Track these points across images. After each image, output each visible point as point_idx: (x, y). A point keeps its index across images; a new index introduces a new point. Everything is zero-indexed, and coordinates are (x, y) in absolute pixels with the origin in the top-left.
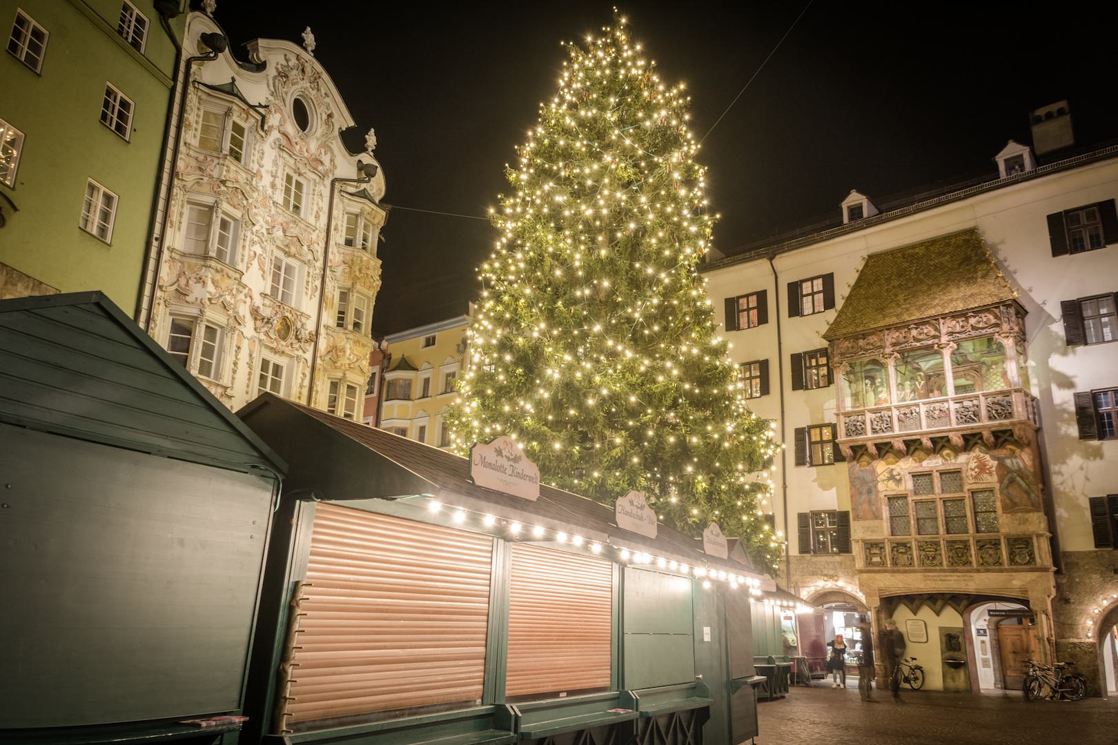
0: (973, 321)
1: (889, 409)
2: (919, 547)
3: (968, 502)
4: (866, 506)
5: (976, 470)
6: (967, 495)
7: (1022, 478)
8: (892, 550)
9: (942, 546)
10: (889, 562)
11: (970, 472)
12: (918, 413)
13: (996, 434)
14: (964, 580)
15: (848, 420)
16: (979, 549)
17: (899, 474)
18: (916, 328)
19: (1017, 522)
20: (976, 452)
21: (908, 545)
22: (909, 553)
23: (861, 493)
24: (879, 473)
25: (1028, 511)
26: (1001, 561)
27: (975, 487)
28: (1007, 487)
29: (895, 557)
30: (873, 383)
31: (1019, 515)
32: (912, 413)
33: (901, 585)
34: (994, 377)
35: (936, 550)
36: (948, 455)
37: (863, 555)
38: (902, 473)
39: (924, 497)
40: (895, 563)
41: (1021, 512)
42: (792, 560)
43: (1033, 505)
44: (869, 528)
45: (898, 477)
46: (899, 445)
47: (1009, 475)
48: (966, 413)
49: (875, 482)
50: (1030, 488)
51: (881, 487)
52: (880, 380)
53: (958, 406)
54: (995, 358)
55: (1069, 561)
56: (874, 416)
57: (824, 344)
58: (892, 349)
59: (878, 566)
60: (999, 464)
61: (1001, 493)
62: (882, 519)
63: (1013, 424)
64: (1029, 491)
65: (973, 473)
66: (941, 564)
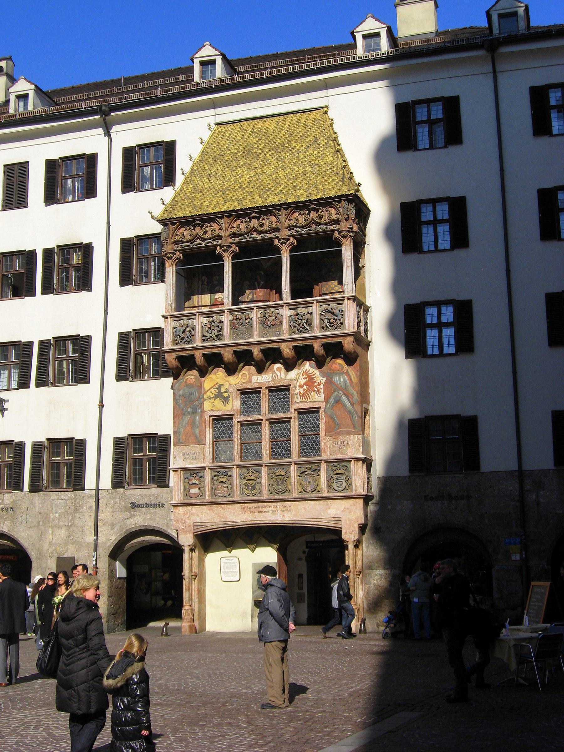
0: (313, 215)
1: (222, 313)
2: (240, 474)
3: (294, 425)
5: (305, 387)
6: (293, 414)
7: (347, 397)
8: (212, 479)
9: (263, 474)
10: (207, 494)
12: (251, 319)
13: (325, 346)
14: (282, 511)
15: (175, 324)
16: (300, 476)
17: (227, 391)
18: (258, 218)
20: (308, 366)
21: (229, 474)
22: (229, 482)
23: (184, 414)
24: (206, 390)
25: (349, 434)
26: (318, 488)
27: (302, 406)
28: (333, 406)
31: (341, 437)
32: (246, 319)
36: (278, 369)
38: (231, 390)
40: (214, 494)
41: (343, 434)
43: (354, 427)
44: (190, 454)
45: (225, 395)
47: (336, 393)
48: (299, 322)
49: (201, 400)
50: (353, 407)
51: (207, 406)
52: (218, 277)
53: (292, 312)
56: (205, 320)
57: (158, 228)
58: (231, 241)
60: (326, 382)
62: (205, 444)
64: (352, 411)
65: (302, 391)
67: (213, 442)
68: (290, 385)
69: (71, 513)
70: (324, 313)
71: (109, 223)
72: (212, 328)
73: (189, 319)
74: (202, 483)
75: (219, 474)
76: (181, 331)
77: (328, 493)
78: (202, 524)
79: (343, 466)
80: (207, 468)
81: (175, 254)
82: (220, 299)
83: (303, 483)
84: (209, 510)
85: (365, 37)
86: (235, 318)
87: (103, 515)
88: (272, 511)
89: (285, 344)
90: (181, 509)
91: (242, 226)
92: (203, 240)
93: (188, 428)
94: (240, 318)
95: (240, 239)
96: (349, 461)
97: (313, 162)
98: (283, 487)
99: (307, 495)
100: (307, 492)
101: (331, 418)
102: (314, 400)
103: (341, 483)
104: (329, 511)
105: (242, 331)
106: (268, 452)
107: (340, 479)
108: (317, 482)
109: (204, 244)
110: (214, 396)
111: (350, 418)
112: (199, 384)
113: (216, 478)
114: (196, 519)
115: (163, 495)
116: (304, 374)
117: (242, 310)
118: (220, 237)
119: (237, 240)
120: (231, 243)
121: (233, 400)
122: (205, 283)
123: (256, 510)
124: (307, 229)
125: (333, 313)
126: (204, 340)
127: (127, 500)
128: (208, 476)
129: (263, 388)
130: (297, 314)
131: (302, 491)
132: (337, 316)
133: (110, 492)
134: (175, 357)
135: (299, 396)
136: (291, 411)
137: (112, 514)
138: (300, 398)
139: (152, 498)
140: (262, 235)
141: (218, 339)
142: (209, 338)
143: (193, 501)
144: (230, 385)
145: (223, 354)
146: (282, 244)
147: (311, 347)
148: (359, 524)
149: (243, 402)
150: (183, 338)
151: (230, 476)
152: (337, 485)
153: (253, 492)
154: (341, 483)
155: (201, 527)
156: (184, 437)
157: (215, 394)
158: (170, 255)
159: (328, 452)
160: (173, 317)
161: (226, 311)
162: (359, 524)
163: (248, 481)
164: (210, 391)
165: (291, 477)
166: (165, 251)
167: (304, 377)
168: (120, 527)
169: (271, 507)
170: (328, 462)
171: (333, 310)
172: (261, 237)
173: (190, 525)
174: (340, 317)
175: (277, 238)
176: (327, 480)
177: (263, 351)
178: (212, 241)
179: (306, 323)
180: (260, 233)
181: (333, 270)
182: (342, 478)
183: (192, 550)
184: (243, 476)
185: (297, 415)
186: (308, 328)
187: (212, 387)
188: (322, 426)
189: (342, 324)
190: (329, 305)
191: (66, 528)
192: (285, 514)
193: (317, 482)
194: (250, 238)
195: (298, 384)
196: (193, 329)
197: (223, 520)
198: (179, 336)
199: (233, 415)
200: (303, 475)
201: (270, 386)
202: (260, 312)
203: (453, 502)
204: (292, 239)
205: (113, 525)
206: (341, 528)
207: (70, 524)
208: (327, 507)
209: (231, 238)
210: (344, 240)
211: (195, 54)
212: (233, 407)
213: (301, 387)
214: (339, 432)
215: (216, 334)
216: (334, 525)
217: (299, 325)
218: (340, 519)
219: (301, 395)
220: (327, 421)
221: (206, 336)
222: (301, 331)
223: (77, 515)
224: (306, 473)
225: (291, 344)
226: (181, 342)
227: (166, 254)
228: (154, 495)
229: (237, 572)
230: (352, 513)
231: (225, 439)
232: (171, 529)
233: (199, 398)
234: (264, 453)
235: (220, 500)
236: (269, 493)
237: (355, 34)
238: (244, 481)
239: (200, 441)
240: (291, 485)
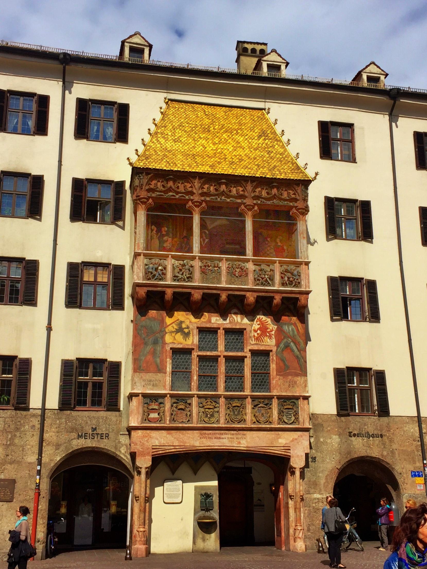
0: (275, 191)
1: (193, 258)
2: (199, 404)
3: (248, 362)
4: (149, 357)
5: (259, 332)
6: (249, 355)
7: (295, 343)
8: (172, 406)
11: (253, 334)
12: (219, 268)
14: (237, 438)
16: (253, 409)
17: (188, 328)
18: (226, 185)
19: (288, 384)
21: (188, 402)
22: (188, 409)
23: (146, 344)
24: (168, 324)
25: (297, 375)
26: (270, 420)
27: (256, 348)
28: (283, 350)
29: (174, 414)
30: (159, 231)
31: (290, 377)
32: (215, 267)
33: (176, 443)
34: (269, 248)
35: (215, 407)
37: (141, 410)
38: (191, 326)
39: (208, 353)
40: (173, 420)
41: (291, 375)
42: (48, 413)
43: (301, 369)
44: (150, 381)
45: (186, 331)
46: (197, 295)
47: (285, 340)
50: (300, 353)
51: (168, 338)
52: (166, 229)
53: (257, 268)
54: (270, 232)
55: (316, 422)
56: (177, 263)
58: (203, 198)
59: (155, 422)
60: (278, 330)
61: (276, 355)
62: (166, 373)
63: (301, 293)
64: (299, 357)
66: (218, 421)
67: (172, 371)
68: (245, 329)
69: (10, 432)
70: (284, 272)
71: (61, 162)
72: (183, 270)
73: (160, 259)
74: (161, 409)
75: (179, 402)
76: (154, 269)
77: (279, 424)
78: (160, 447)
79: (291, 402)
80: (168, 395)
81: (148, 201)
82: (168, 247)
83: (257, 414)
84: (169, 434)
85: (269, 66)
86: (205, 264)
87: (48, 435)
88: (228, 438)
89: (250, 293)
90: (140, 432)
91: (212, 188)
92: (177, 193)
93: (149, 357)
94: (210, 265)
95: (212, 199)
96: (297, 398)
97: (266, 149)
98: (239, 417)
99: (260, 426)
100: (260, 423)
101: (281, 360)
102: (267, 344)
103: (290, 416)
104: (280, 441)
105: (211, 277)
106: (224, 384)
107: (289, 413)
108: (269, 414)
109: (177, 196)
110: (175, 330)
111: (298, 362)
112: (161, 318)
113: (175, 405)
114: (155, 442)
115: (112, 417)
116: (258, 321)
117: (212, 259)
118: (192, 193)
119: (208, 199)
120: (203, 201)
121: (193, 336)
122: (154, 232)
123: (214, 436)
124: (272, 201)
125: (292, 274)
126: (175, 280)
127: (74, 421)
128: (168, 403)
129: (221, 328)
130: (261, 270)
131: (256, 421)
132: (295, 276)
133: (56, 412)
134: (146, 291)
135: (253, 339)
136: (245, 350)
137: (57, 434)
138: (255, 341)
139: (101, 420)
140: (231, 199)
141: (189, 281)
142: (180, 279)
143: (155, 425)
144: (190, 322)
145: (193, 294)
146: (248, 210)
147: (273, 298)
148: (306, 454)
149: (200, 338)
150: (154, 275)
151: (190, 404)
152: (287, 418)
153: (211, 420)
154: (290, 416)
155: (159, 450)
156: (145, 365)
157: (176, 329)
158: (145, 200)
159: (279, 389)
160: (145, 255)
161: (197, 258)
162: (306, 454)
163: (207, 410)
164: (171, 325)
165: (246, 408)
166: (139, 196)
167: (258, 323)
168: (66, 447)
169: (228, 434)
170: (279, 398)
171: (292, 270)
172: (230, 200)
173: (149, 448)
174: (298, 277)
175: (244, 204)
176: (278, 413)
177: (229, 296)
178: (185, 195)
179: (270, 279)
180: (228, 196)
181: (269, 239)
182: (291, 413)
183: (147, 473)
184: (201, 405)
185: (250, 355)
186: (270, 282)
187: (173, 323)
188: (273, 366)
189: (299, 283)
190: (288, 266)
191: (4, 447)
192: (241, 442)
193: (269, 414)
194: (221, 199)
195: (253, 328)
196: (165, 268)
197: (182, 444)
198: (152, 273)
199: (193, 349)
200: (256, 409)
201: (228, 327)
202: (228, 263)
203: (371, 438)
204: (256, 208)
205: (58, 446)
206: (290, 456)
207: (8, 443)
208: (279, 436)
209: (202, 196)
210: (301, 216)
211: (129, 38)
212: (193, 342)
213: (255, 331)
214: (288, 373)
215: (188, 276)
216: (283, 453)
217: (262, 278)
218: (289, 448)
219: (255, 338)
220: (278, 362)
221: (177, 277)
222: (264, 285)
223: (18, 434)
224: (259, 406)
225: (255, 295)
226: (152, 278)
227: (139, 199)
228: (102, 418)
229: (180, 494)
230: (300, 443)
231: (183, 370)
232: (120, 451)
233: (161, 331)
234: (222, 385)
235: (180, 425)
236: (227, 421)
237: (262, 62)
238: (202, 410)
239: (161, 369)
240: (246, 416)
